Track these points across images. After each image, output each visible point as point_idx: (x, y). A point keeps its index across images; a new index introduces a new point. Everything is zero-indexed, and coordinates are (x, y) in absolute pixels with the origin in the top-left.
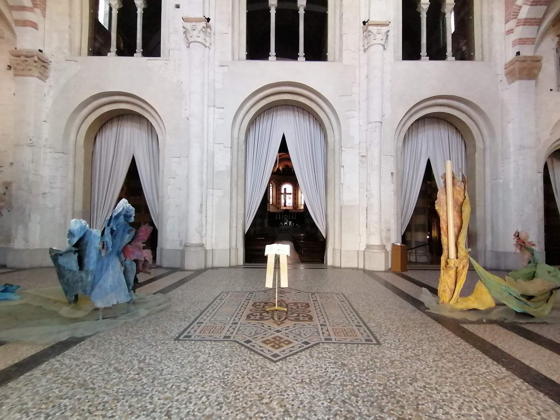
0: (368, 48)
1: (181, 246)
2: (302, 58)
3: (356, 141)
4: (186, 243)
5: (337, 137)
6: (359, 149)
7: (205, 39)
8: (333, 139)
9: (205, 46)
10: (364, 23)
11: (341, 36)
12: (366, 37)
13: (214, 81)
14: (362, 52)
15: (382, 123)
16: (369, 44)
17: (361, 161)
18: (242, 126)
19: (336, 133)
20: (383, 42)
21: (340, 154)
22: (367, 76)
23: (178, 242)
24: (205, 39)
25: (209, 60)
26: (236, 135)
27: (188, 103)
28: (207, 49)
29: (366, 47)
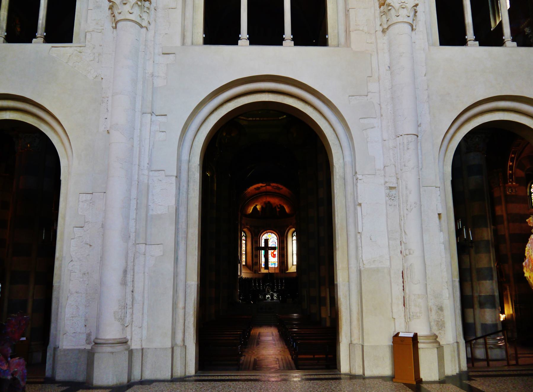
0: (387, 28)
1: (89, 344)
2: (288, 43)
3: (379, 165)
4: (96, 338)
6: (385, 176)
7: (141, 17)
8: (341, 161)
9: (142, 27)
11: (347, 12)
12: (384, 13)
13: (152, 75)
14: (380, 33)
15: (418, 136)
16: (389, 23)
17: (388, 195)
18: (195, 143)
19: (347, 152)
20: (410, 20)
21: (355, 185)
22: (389, 67)
23: (84, 337)
24: (141, 17)
25: (146, 45)
26: (185, 157)
27: (110, 109)
28: (144, 30)
29: (386, 27)
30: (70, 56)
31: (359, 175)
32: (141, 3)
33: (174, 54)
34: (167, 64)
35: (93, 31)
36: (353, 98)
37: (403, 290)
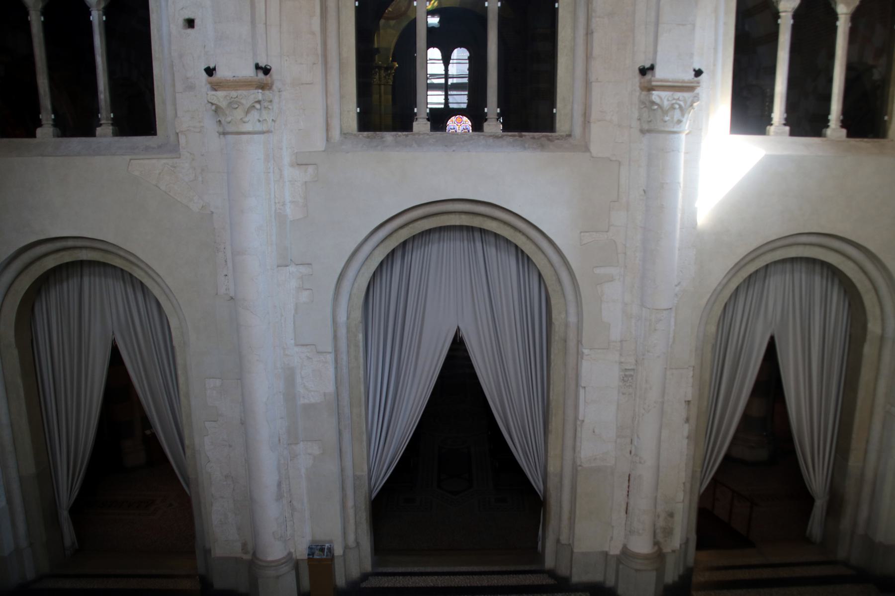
3: (616, 334)
5: (572, 319)
8: (563, 316)
10: (643, 71)
11: (588, 84)
19: (572, 310)
22: (644, 191)
30: (160, 174)
31: (585, 349)
32: (260, 105)
33: (315, 164)
34: (306, 182)
35: (188, 130)
36: (587, 234)
37: (628, 495)
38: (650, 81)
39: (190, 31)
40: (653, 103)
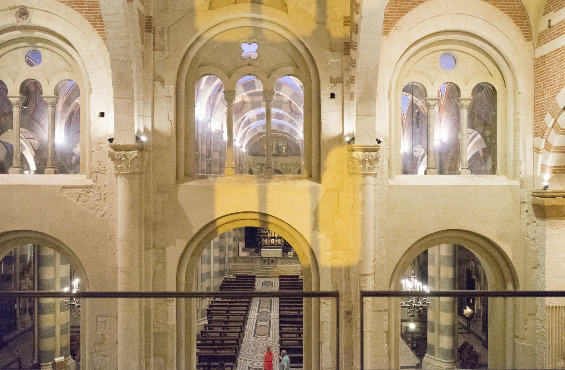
38: (352, 147)
39: (102, 118)
40: (355, 158)
